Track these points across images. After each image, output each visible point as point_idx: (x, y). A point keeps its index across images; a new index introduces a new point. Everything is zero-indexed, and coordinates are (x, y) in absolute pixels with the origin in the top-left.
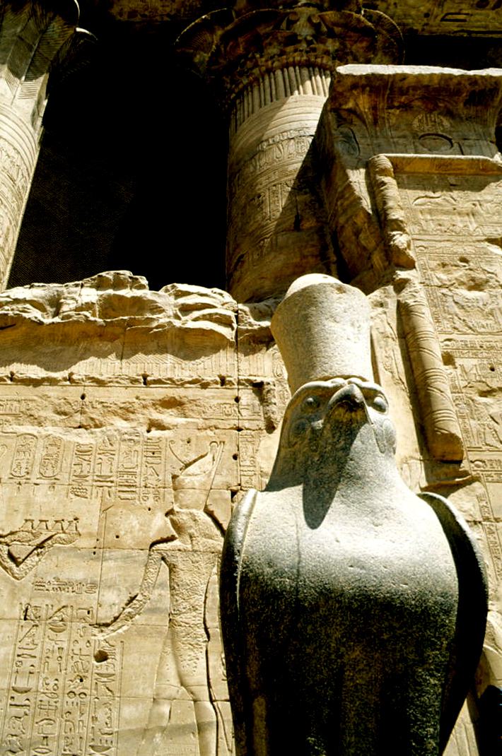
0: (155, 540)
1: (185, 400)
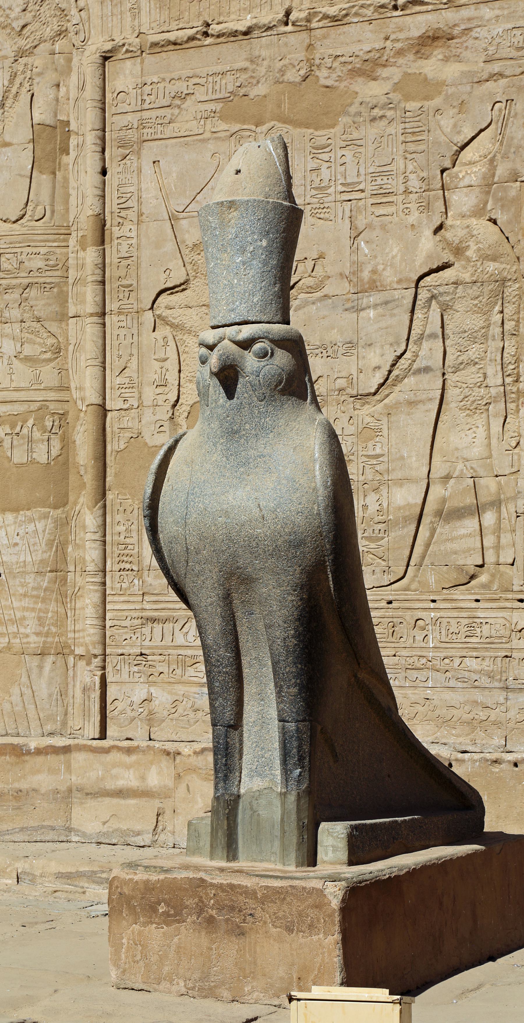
1: (456, 32)
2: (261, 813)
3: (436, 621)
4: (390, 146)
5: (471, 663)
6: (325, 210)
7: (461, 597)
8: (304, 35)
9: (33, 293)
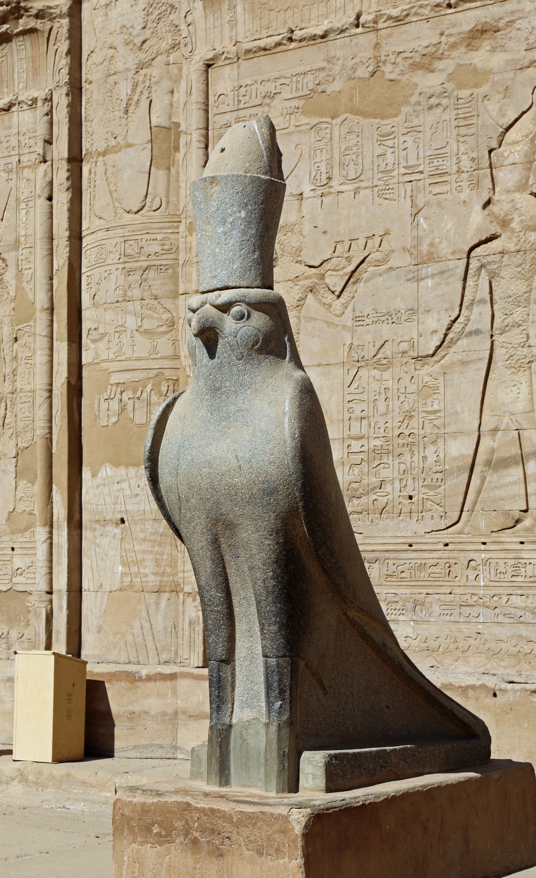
0: (472, 245)
1: (501, 24)
2: (249, 741)
3: (486, 562)
4: (445, 130)
5: (516, 600)
6: (390, 191)
7: (508, 540)
8: (372, 35)
9: (151, 274)
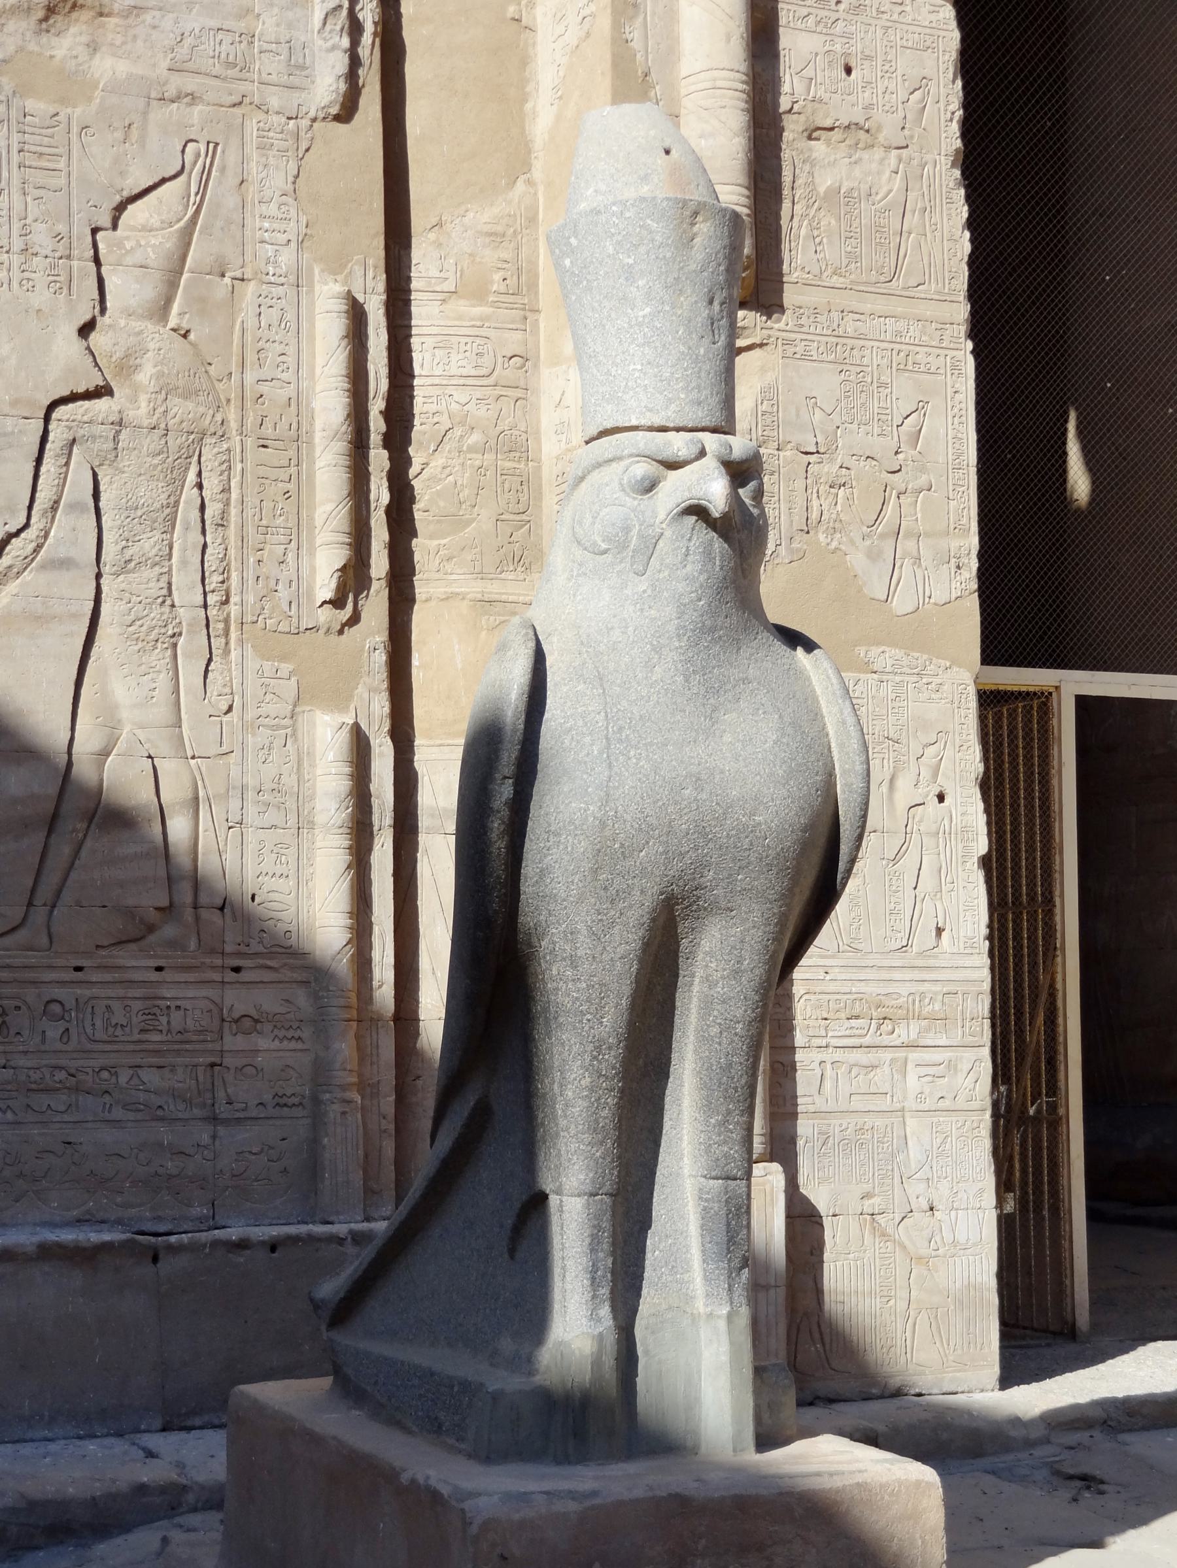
0: (57, 397)
